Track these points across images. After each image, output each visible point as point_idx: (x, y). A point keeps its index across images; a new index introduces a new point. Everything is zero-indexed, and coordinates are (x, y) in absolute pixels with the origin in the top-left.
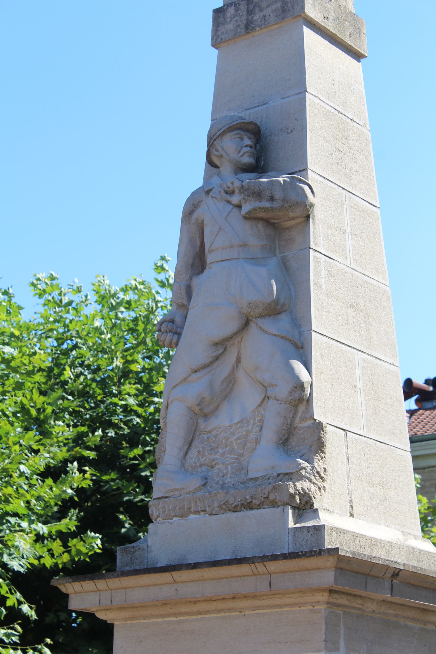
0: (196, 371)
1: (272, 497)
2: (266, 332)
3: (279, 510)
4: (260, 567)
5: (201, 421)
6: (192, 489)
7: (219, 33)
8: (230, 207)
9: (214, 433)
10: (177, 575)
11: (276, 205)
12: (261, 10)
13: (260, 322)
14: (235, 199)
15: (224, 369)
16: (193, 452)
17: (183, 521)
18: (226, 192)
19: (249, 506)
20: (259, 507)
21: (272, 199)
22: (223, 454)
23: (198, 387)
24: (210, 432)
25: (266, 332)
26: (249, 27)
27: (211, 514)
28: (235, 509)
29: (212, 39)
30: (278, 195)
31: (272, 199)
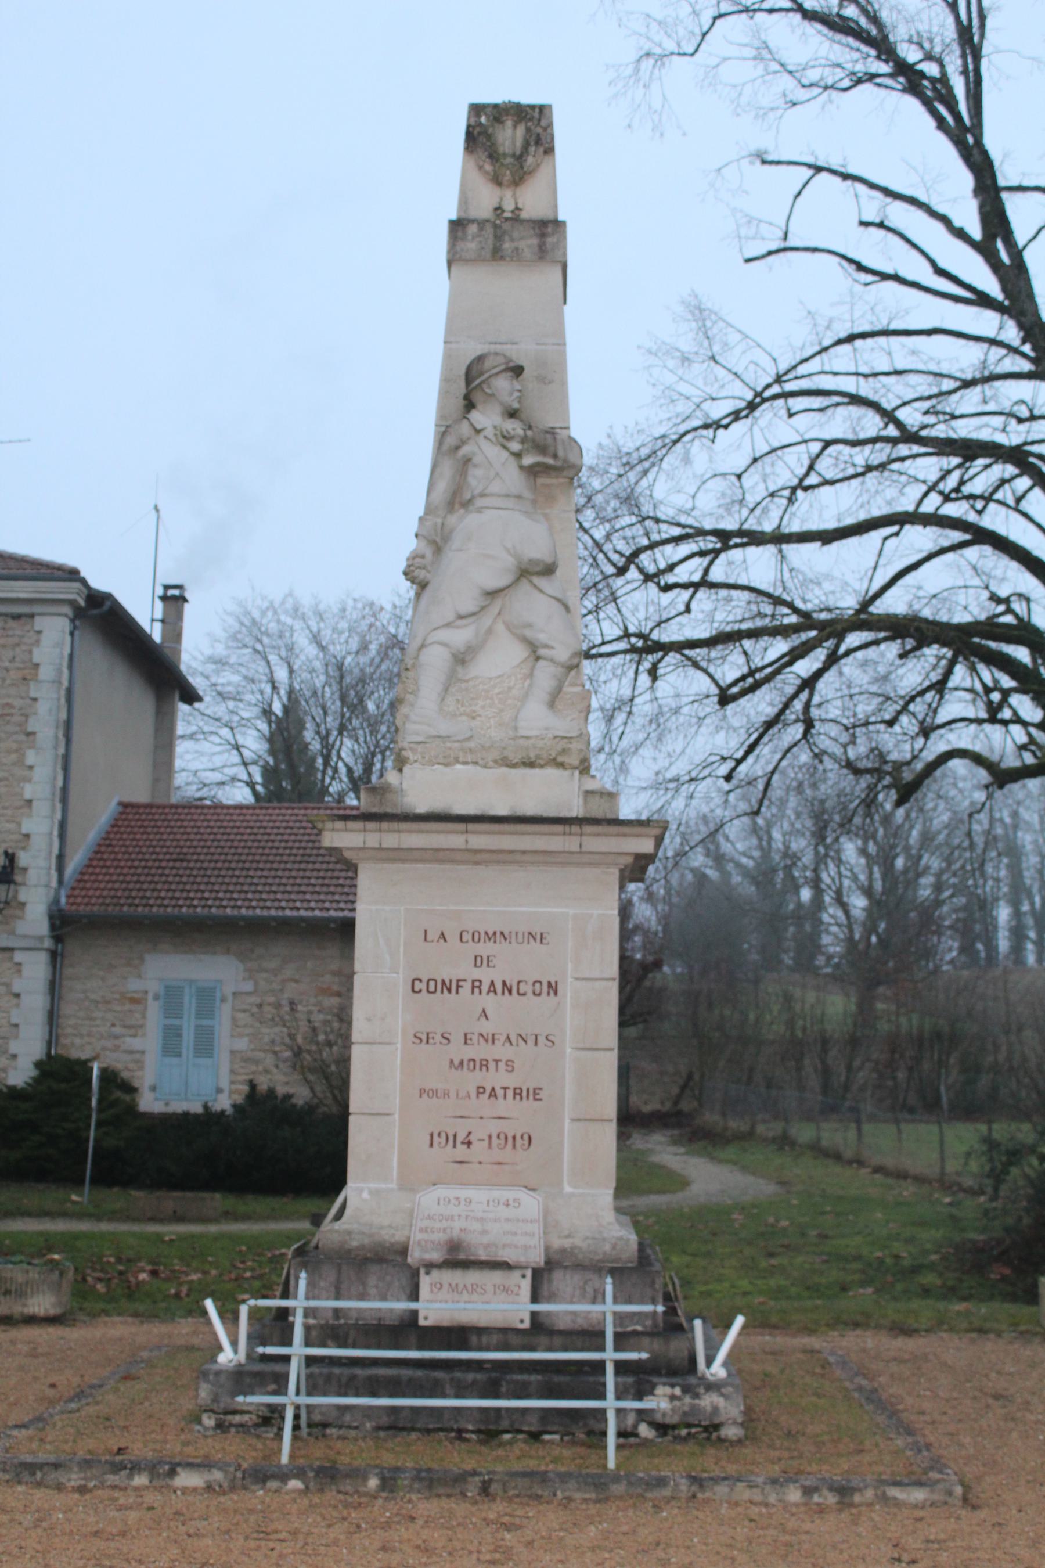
0: (461, 617)
1: (560, 759)
2: (541, 591)
3: (567, 773)
4: (575, 829)
5: (459, 669)
6: (460, 738)
7: (458, 248)
8: (505, 454)
9: (471, 683)
10: (471, 826)
11: (559, 463)
12: (512, 240)
13: (536, 580)
14: (515, 446)
15: (487, 621)
16: (450, 701)
17: (448, 770)
18: (504, 437)
19: (531, 764)
20: (542, 766)
21: (555, 456)
22: (483, 707)
23: (461, 637)
24: (467, 681)
25: (541, 591)
26: (497, 255)
27: (485, 767)
28: (514, 766)
29: (449, 252)
30: (561, 453)
31: (555, 456)
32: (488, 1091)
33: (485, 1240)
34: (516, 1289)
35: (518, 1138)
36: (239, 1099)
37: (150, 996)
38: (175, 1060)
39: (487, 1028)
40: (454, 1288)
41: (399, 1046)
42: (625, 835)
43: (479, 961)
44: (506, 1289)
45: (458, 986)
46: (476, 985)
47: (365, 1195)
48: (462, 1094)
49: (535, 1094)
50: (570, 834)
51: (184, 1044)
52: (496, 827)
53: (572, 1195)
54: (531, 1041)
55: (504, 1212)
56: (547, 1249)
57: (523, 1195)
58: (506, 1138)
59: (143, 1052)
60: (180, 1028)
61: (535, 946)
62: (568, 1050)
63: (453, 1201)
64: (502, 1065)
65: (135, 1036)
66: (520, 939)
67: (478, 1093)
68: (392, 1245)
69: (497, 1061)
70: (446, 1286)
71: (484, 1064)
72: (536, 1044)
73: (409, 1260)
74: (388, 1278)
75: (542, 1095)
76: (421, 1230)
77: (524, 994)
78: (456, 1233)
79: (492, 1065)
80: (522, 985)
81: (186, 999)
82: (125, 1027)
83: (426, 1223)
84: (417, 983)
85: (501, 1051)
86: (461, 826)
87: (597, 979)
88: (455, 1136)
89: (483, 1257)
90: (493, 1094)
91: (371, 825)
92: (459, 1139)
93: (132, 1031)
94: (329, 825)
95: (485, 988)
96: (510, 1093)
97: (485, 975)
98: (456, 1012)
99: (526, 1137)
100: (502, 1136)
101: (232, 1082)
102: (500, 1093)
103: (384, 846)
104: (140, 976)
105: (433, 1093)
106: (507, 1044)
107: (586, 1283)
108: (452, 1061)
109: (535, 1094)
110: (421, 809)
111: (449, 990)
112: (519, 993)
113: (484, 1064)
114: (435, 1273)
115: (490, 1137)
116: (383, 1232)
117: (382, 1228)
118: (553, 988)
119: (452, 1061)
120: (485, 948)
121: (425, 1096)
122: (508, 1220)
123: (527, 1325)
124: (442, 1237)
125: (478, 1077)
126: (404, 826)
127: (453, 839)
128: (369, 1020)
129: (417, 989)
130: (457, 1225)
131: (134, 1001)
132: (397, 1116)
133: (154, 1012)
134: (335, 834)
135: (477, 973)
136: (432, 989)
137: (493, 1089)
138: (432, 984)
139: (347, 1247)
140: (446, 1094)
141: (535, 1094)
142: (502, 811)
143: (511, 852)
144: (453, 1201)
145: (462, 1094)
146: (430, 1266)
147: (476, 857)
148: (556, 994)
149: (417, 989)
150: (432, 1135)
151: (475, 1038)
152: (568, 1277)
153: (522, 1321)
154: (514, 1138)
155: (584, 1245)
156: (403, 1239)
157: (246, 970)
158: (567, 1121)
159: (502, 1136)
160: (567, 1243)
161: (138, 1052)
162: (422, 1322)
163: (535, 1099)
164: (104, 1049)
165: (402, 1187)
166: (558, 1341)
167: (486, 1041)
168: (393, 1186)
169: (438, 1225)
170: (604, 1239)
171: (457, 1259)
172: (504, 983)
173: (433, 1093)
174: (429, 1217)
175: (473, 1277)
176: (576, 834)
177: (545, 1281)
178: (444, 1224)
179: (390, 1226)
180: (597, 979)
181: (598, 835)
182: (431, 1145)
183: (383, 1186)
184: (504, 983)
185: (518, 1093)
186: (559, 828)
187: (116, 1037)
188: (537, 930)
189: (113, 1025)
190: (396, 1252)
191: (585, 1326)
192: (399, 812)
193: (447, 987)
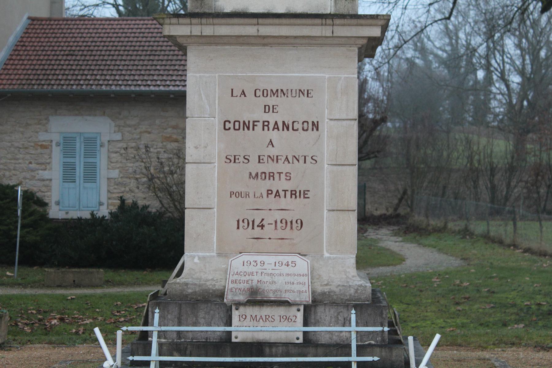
4: (329, 21)
10: (260, 21)
32: (274, 193)
33: (274, 287)
34: (294, 319)
35: (294, 222)
36: (114, 209)
37: (54, 144)
38: (72, 185)
39: (273, 152)
40: (254, 318)
41: (216, 164)
42: (362, 25)
43: (267, 109)
44: (287, 319)
45: (254, 125)
46: (266, 124)
47: (196, 260)
48: (257, 195)
49: (305, 194)
50: (326, 25)
51: (77, 174)
52: (277, 21)
53: (329, 258)
54: (302, 160)
55: (285, 270)
56: (313, 292)
58: (286, 222)
59: (51, 180)
60: (74, 164)
61: (304, 98)
62: (326, 166)
63: (253, 263)
64: (283, 176)
65: (45, 170)
66: (294, 95)
67: (268, 194)
68: (214, 291)
69: (280, 173)
70: (249, 317)
71: (271, 176)
72: (305, 162)
73: (225, 300)
74: (212, 312)
75: (309, 195)
76: (232, 282)
77: (297, 130)
78: (255, 283)
79: (276, 176)
80: (295, 124)
81: (78, 145)
82: (38, 164)
83: (235, 277)
84: (227, 123)
85: (282, 167)
86: (255, 21)
87: (344, 120)
88: (253, 221)
89: (272, 297)
90: (277, 194)
91: (194, 21)
92: (256, 224)
93: (43, 166)
94: (167, 21)
95: (271, 126)
96: (288, 194)
97: (271, 118)
98: (253, 142)
99: (299, 222)
100: (284, 221)
101: (109, 199)
102: (282, 194)
103: (204, 34)
104: (46, 131)
105: (239, 194)
106: (286, 162)
107: (338, 314)
108: (250, 174)
109: (304, 194)
110: (228, 10)
111: (248, 128)
112: (293, 129)
113: (271, 176)
114: (242, 309)
115: (276, 222)
116: (208, 283)
117: (207, 280)
118: (316, 126)
119: (250, 174)
120: (271, 101)
121: (233, 196)
122: (288, 275)
123: (301, 341)
124: (247, 286)
125: (268, 184)
126: (216, 21)
127: (249, 29)
128: (196, 148)
129: (227, 128)
130: (255, 278)
131: (43, 147)
132: (215, 210)
133: (57, 154)
134: (172, 27)
135: (266, 117)
136: (237, 127)
137: (278, 191)
138: (237, 124)
139: (184, 293)
140: (247, 195)
141: (305, 194)
142: (281, 10)
143: (287, 37)
144: (253, 263)
145: (257, 195)
146: (238, 305)
147: (264, 41)
148: (317, 130)
149: (227, 128)
150: (238, 221)
151: (265, 159)
152: (327, 310)
153: (298, 339)
154: (291, 222)
155: (337, 290)
156: (221, 288)
157: (115, 126)
158: (326, 211)
159: (284, 221)
160: (326, 289)
161: (47, 180)
162: (234, 340)
163: (305, 197)
164: (25, 178)
165: (219, 255)
166: (320, 350)
167: (273, 160)
168: (215, 254)
169: (243, 278)
170: (350, 286)
171: (256, 299)
172: (284, 122)
173: (239, 194)
175: (266, 311)
176: (329, 25)
177: (312, 313)
178: (247, 278)
179: (212, 280)
180: (344, 120)
181: (344, 25)
182: (238, 228)
183: (208, 254)
184: (284, 122)
185: (293, 193)
186: (318, 21)
187: (32, 171)
188: (304, 88)
189: (30, 163)
190: (217, 296)
191: (338, 341)
192: (213, 12)
193: (246, 126)
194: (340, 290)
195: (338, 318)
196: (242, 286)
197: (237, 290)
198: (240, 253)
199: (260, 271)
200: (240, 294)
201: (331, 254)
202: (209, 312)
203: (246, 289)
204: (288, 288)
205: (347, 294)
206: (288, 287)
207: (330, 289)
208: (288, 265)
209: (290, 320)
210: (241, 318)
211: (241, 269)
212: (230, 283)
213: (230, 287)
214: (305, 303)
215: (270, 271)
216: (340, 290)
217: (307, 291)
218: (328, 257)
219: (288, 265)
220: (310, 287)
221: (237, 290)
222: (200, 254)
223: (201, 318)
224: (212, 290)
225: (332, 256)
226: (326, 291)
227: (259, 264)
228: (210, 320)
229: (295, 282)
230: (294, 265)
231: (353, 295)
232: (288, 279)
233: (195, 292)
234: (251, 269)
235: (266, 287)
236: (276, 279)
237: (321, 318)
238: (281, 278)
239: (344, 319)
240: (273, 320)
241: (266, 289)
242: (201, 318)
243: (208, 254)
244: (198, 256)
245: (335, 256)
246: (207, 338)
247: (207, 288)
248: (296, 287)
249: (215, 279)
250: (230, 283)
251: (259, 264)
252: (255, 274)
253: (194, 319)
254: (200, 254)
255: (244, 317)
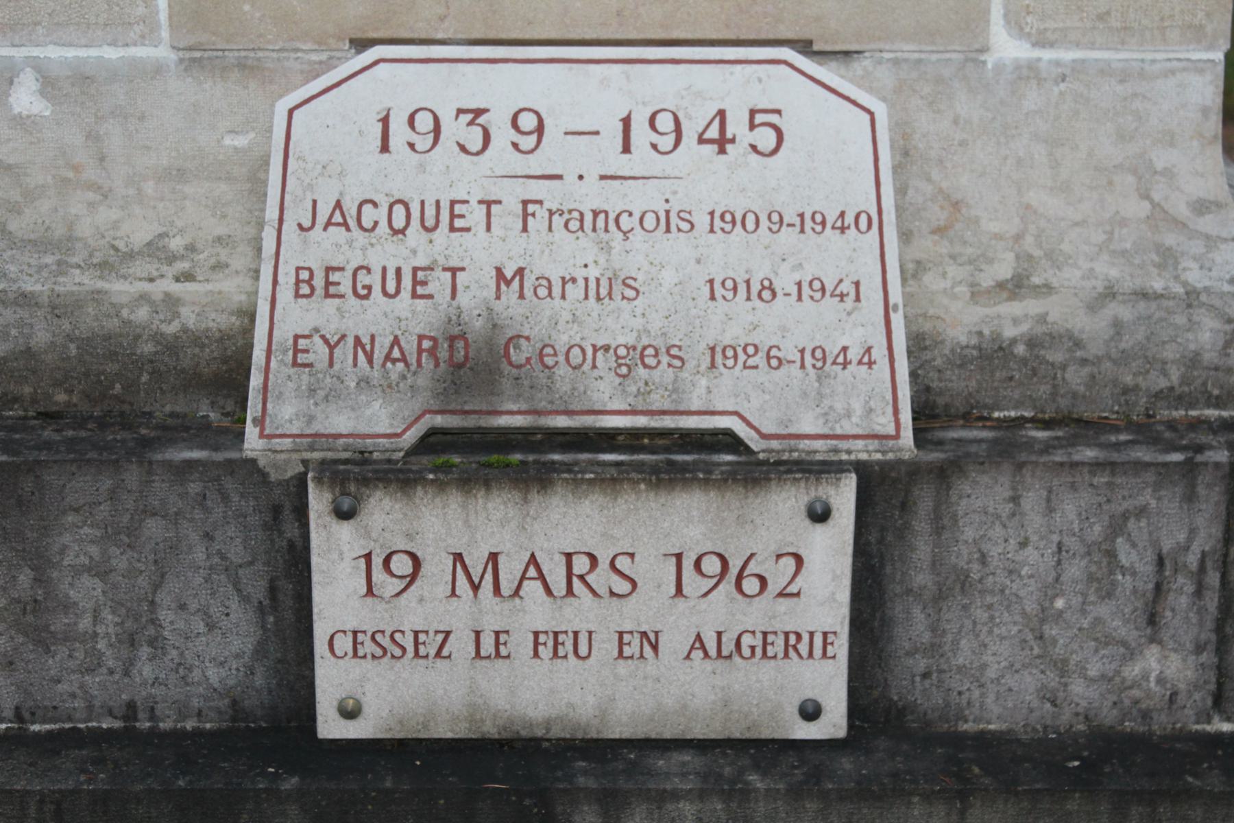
33: (619, 325)
40: (478, 575)
44: (734, 575)
53: (1028, 73)
55: (703, 179)
56: (919, 344)
57: (784, 85)
63: (454, 129)
68: (171, 346)
70: (437, 567)
73: (253, 441)
74: (154, 528)
76: (304, 286)
78: (476, 292)
83: (326, 247)
89: (611, 404)
107: (1117, 527)
116: (120, 289)
117: (113, 262)
123: (833, 723)
130: (480, 253)
144: (454, 129)
152: (1032, 500)
153: (811, 712)
155: (1092, 327)
156: (221, 321)
160: (1013, 319)
162: (330, 726)
165: (198, 60)
168: (162, 52)
169: (386, 254)
170: (1191, 297)
171: (491, 434)
174: (339, 217)
175: (570, 521)
177: (921, 525)
178: (418, 248)
179: (155, 249)
183: (111, 54)
190: (193, 382)
191: (1108, 716)
194: (1117, 324)
195: (1111, 554)
196: (379, 318)
197: (345, 352)
198: (361, 44)
199: (511, 195)
200: (364, 382)
201: (1041, 42)
202: (133, 531)
203: (410, 346)
204: (733, 334)
205: (1170, 353)
206: (733, 322)
207: (1042, 319)
208: (722, 143)
209: (751, 585)
210: (378, 575)
211: (368, 176)
212: (285, 294)
213: (284, 333)
214: (862, 451)
215: (590, 196)
216: (1117, 324)
217: (880, 353)
218: (1018, 66)
219: (722, 143)
220: (898, 320)
221: (345, 352)
222: (53, 52)
223: (77, 571)
224: (157, 337)
225: (1047, 55)
226: (1009, 332)
227: (503, 136)
228: (143, 582)
229: (785, 283)
230: (766, 139)
231: (1209, 357)
232: (732, 254)
233: (28, 352)
234: (447, 175)
235: (561, 323)
236: (637, 254)
237: (983, 559)
238: (676, 247)
239: (1160, 562)
240: (623, 587)
241: (561, 342)
242: (77, 571)
243: (111, 54)
244: (39, 67)
245: (1068, 55)
246: (131, 706)
247: (113, 324)
248: (795, 324)
249: (176, 244)
250: (285, 294)
251: (503, 136)
252: (476, 215)
253: (25, 577)
254: (53, 52)
255: (402, 565)
